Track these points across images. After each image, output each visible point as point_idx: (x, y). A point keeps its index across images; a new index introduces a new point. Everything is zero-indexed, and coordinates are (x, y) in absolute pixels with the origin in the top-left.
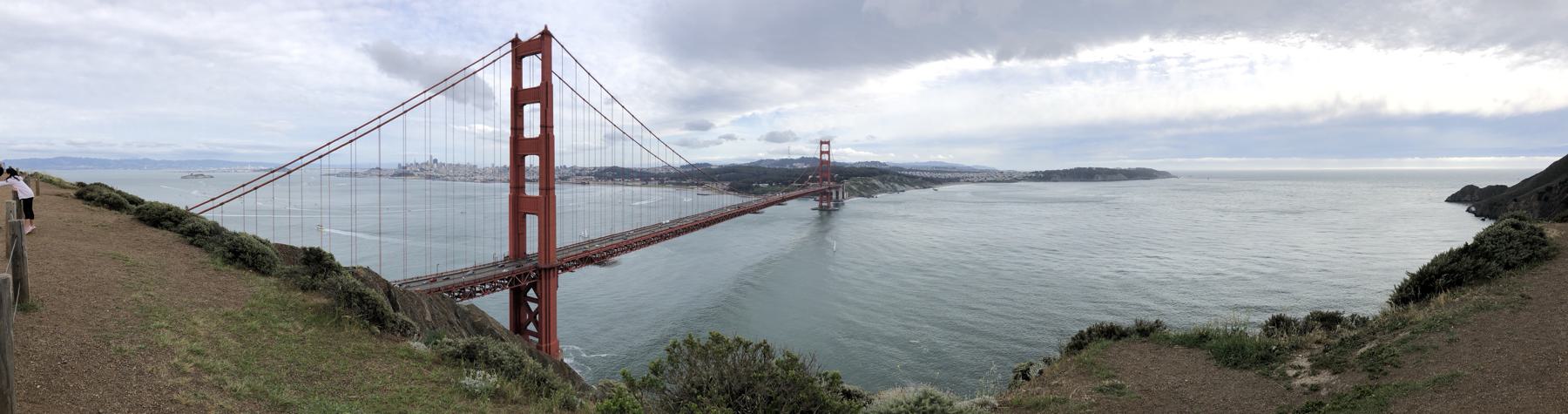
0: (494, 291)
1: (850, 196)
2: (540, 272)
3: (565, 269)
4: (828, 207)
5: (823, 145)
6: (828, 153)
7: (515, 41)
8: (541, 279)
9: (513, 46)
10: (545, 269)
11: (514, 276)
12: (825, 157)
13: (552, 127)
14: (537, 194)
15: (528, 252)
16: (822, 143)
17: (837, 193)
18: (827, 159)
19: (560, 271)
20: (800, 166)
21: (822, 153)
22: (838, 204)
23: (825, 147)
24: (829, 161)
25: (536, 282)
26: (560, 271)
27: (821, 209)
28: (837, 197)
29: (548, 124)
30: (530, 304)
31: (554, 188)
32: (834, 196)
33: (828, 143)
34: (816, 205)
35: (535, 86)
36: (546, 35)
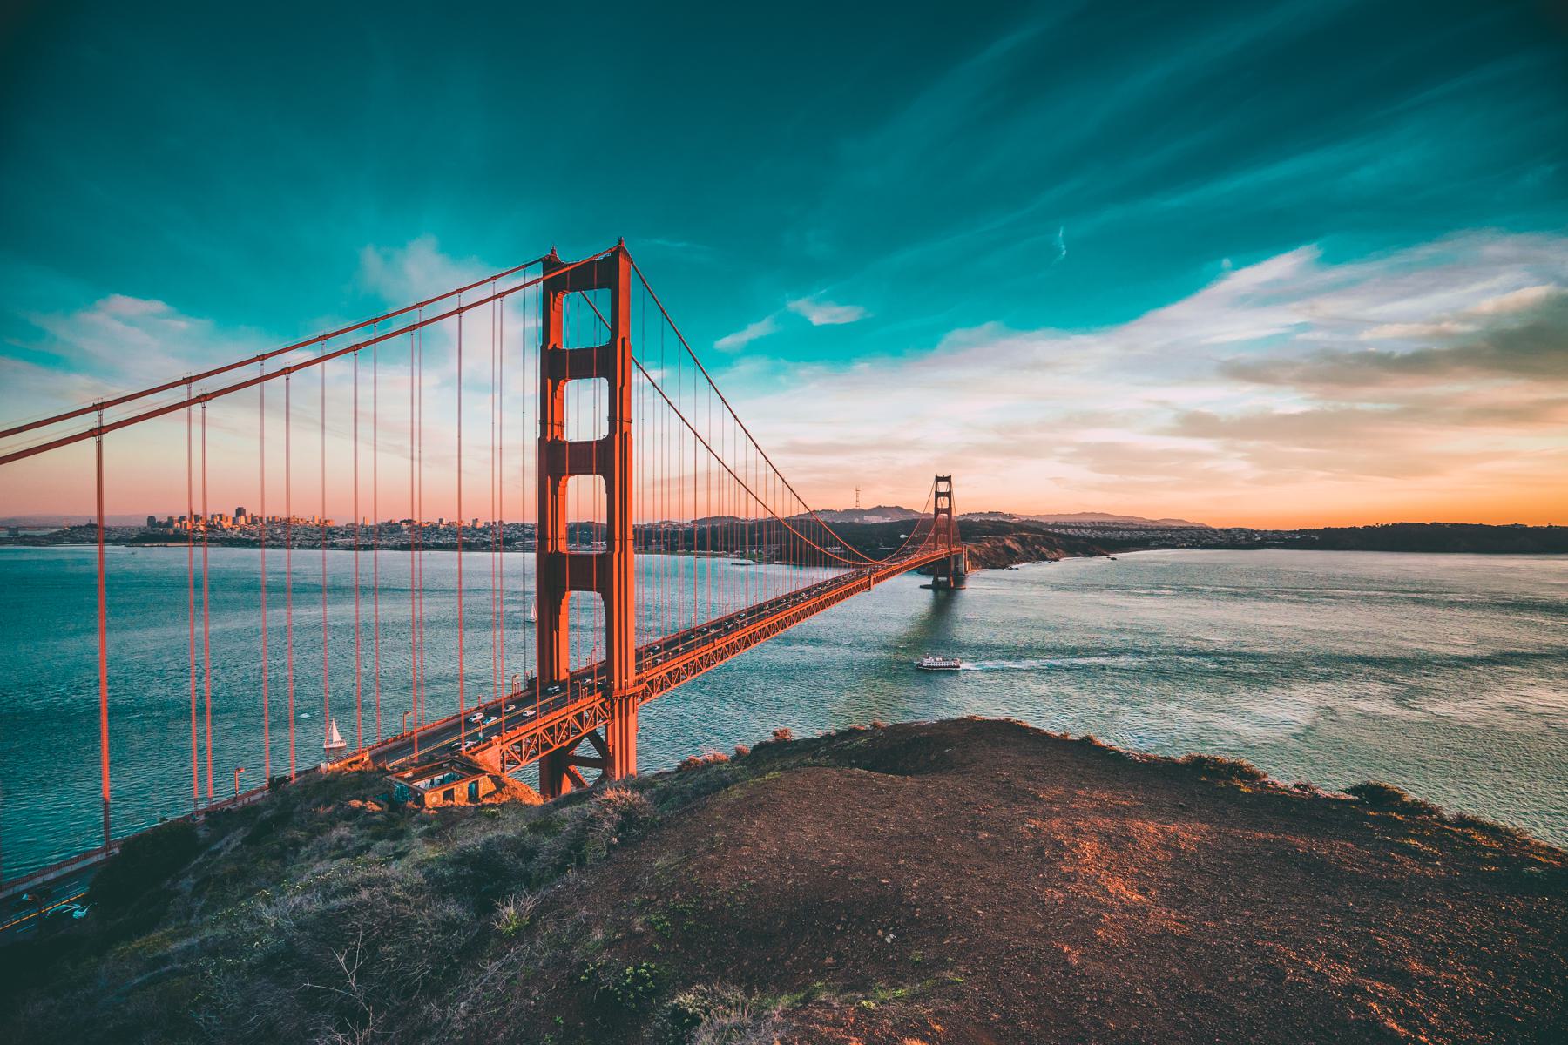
1: (975, 566)
2: (613, 705)
5: (939, 483)
6: (949, 494)
8: (613, 718)
9: (546, 271)
12: (944, 503)
16: (938, 479)
18: (946, 506)
20: (874, 519)
21: (938, 495)
22: (960, 580)
23: (943, 487)
24: (949, 511)
27: (935, 587)
33: (948, 479)
34: (929, 581)
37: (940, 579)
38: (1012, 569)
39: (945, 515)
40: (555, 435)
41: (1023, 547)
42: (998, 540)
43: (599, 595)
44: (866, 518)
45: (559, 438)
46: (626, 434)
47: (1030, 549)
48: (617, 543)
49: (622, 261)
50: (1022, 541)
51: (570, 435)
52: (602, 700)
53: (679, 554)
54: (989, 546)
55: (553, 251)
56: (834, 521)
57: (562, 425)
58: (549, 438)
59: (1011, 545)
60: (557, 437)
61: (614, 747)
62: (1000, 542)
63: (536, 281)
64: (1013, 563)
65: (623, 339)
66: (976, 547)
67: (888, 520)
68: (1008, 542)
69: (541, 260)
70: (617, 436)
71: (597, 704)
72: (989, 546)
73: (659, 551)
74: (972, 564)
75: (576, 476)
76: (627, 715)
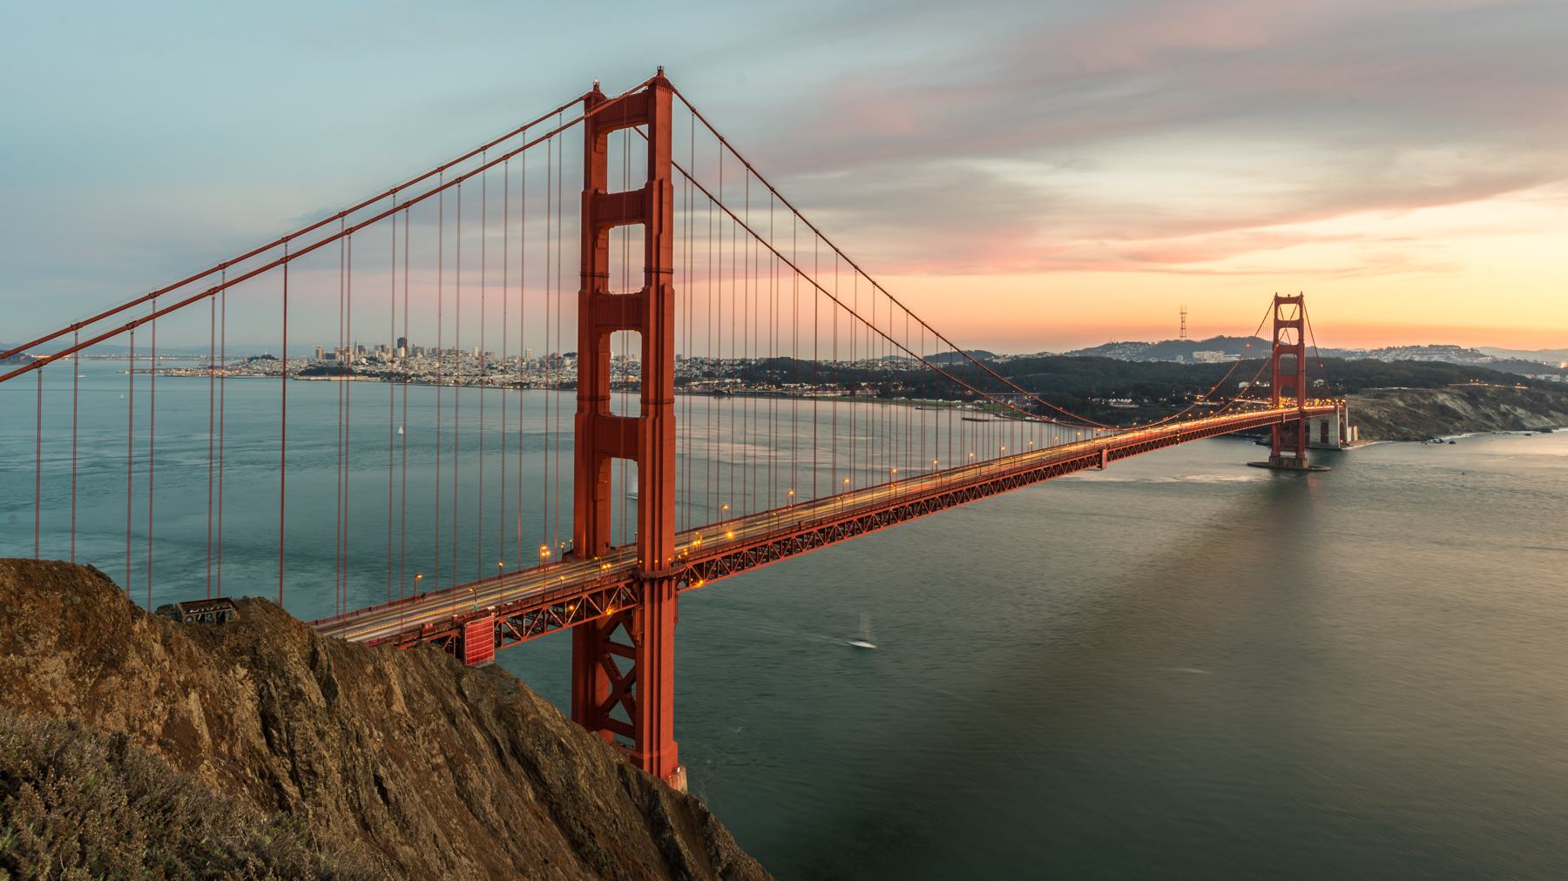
0: (543, 631)
2: (642, 586)
4: (1300, 459)
10: (652, 581)
11: (585, 596)
13: (672, 273)
14: (636, 412)
17: (1325, 428)
25: (628, 612)
27: (1275, 465)
28: (1325, 438)
29: (663, 265)
30: (617, 659)
31: (672, 401)
32: (1315, 435)
34: (1264, 454)
37: (1283, 454)
38: (1441, 441)
39: (1291, 356)
40: (596, 287)
41: (1475, 406)
42: (1421, 394)
44: (1196, 355)
45: (601, 290)
46: (663, 287)
47: (1489, 411)
50: (1472, 397)
51: (615, 287)
52: (629, 581)
53: (897, 403)
54: (1401, 403)
56: (1134, 360)
57: (605, 276)
58: (588, 290)
59: (1449, 404)
60: (598, 290)
61: (643, 635)
62: (1425, 399)
64: (1447, 433)
65: (661, 182)
66: (1373, 405)
67: (1234, 358)
68: (1441, 398)
70: (653, 289)
71: (621, 585)
72: (1401, 403)
73: (868, 399)
74: (1360, 432)
75: (619, 332)
76: (660, 600)
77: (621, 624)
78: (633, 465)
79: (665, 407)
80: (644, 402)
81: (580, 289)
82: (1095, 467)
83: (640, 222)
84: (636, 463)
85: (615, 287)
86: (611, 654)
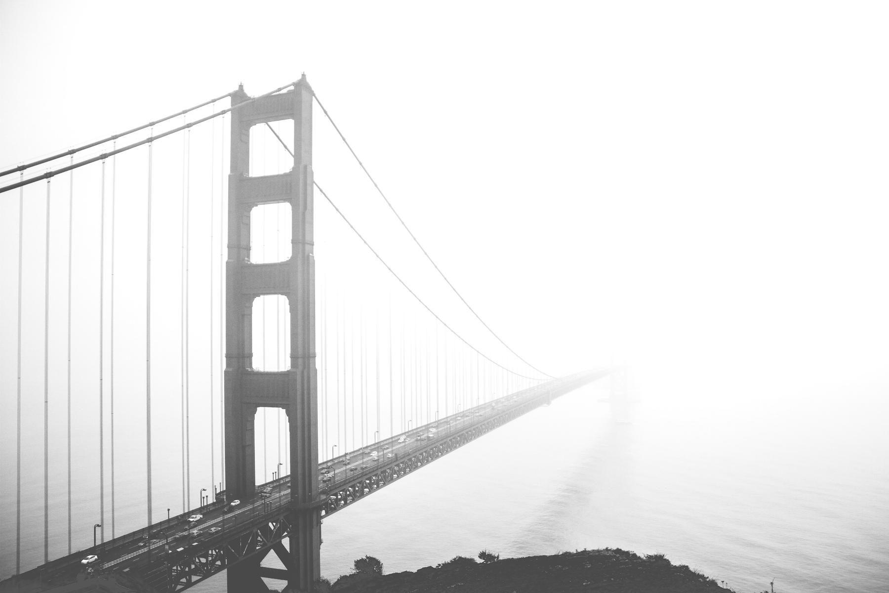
3: (332, 508)
7: (238, 96)
13: (313, 245)
14: (285, 365)
15: (259, 480)
19: (323, 513)
26: (323, 513)
29: (307, 238)
35: (282, 172)
36: (302, 85)
43: (284, 410)
48: (300, 361)
49: (304, 94)
51: (258, 257)
55: (241, 86)
63: (223, 112)
65: (305, 167)
69: (229, 95)
75: (262, 296)
77: (272, 551)
78: (283, 412)
79: (311, 360)
80: (294, 357)
81: (227, 259)
82: (545, 405)
83: (285, 200)
84: (284, 410)
85: (258, 257)
86: (265, 580)
